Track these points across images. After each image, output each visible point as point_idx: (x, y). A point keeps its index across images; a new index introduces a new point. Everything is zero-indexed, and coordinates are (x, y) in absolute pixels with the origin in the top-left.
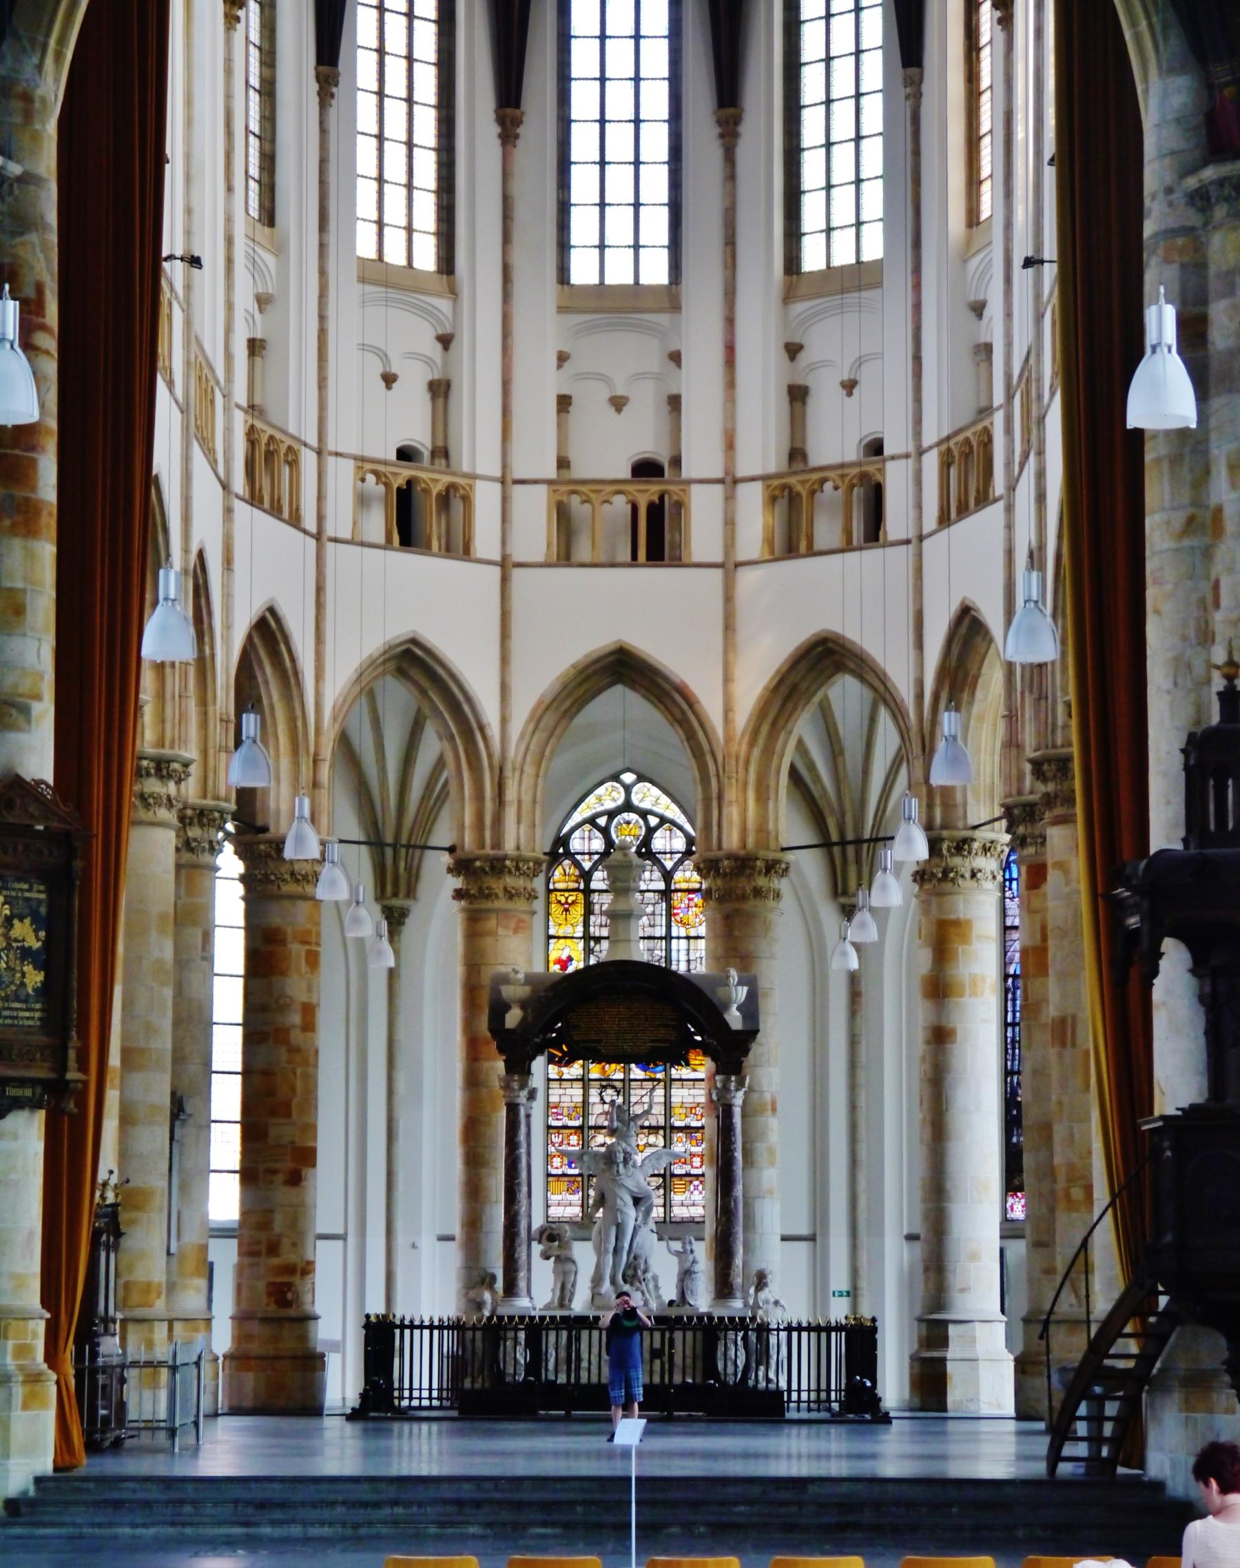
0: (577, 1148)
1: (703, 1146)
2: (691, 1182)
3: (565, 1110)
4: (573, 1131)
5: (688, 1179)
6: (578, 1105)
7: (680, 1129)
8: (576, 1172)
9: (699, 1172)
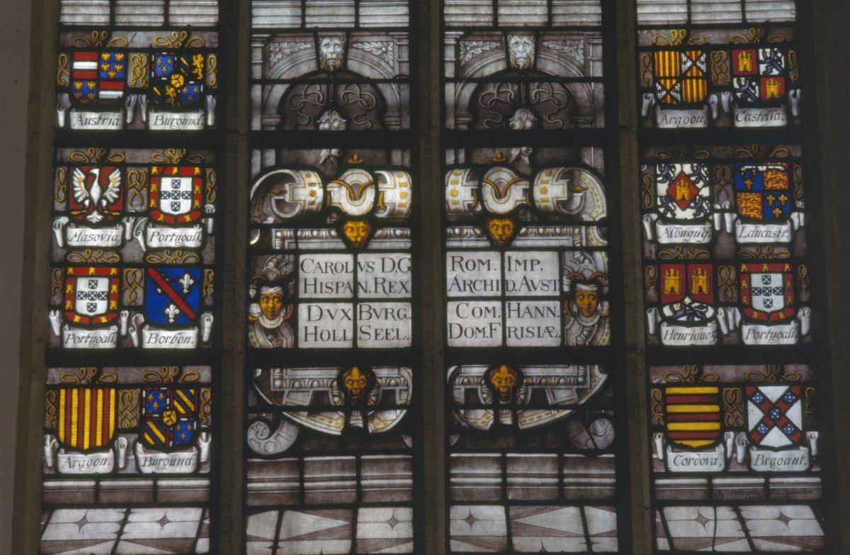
0: (192, 236)
1: (798, 219)
2: (748, 389)
3: (138, 61)
4: (175, 155)
5: (730, 372)
6: (197, 40)
7: (682, 146)
8: (186, 339)
9: (786, 335)
